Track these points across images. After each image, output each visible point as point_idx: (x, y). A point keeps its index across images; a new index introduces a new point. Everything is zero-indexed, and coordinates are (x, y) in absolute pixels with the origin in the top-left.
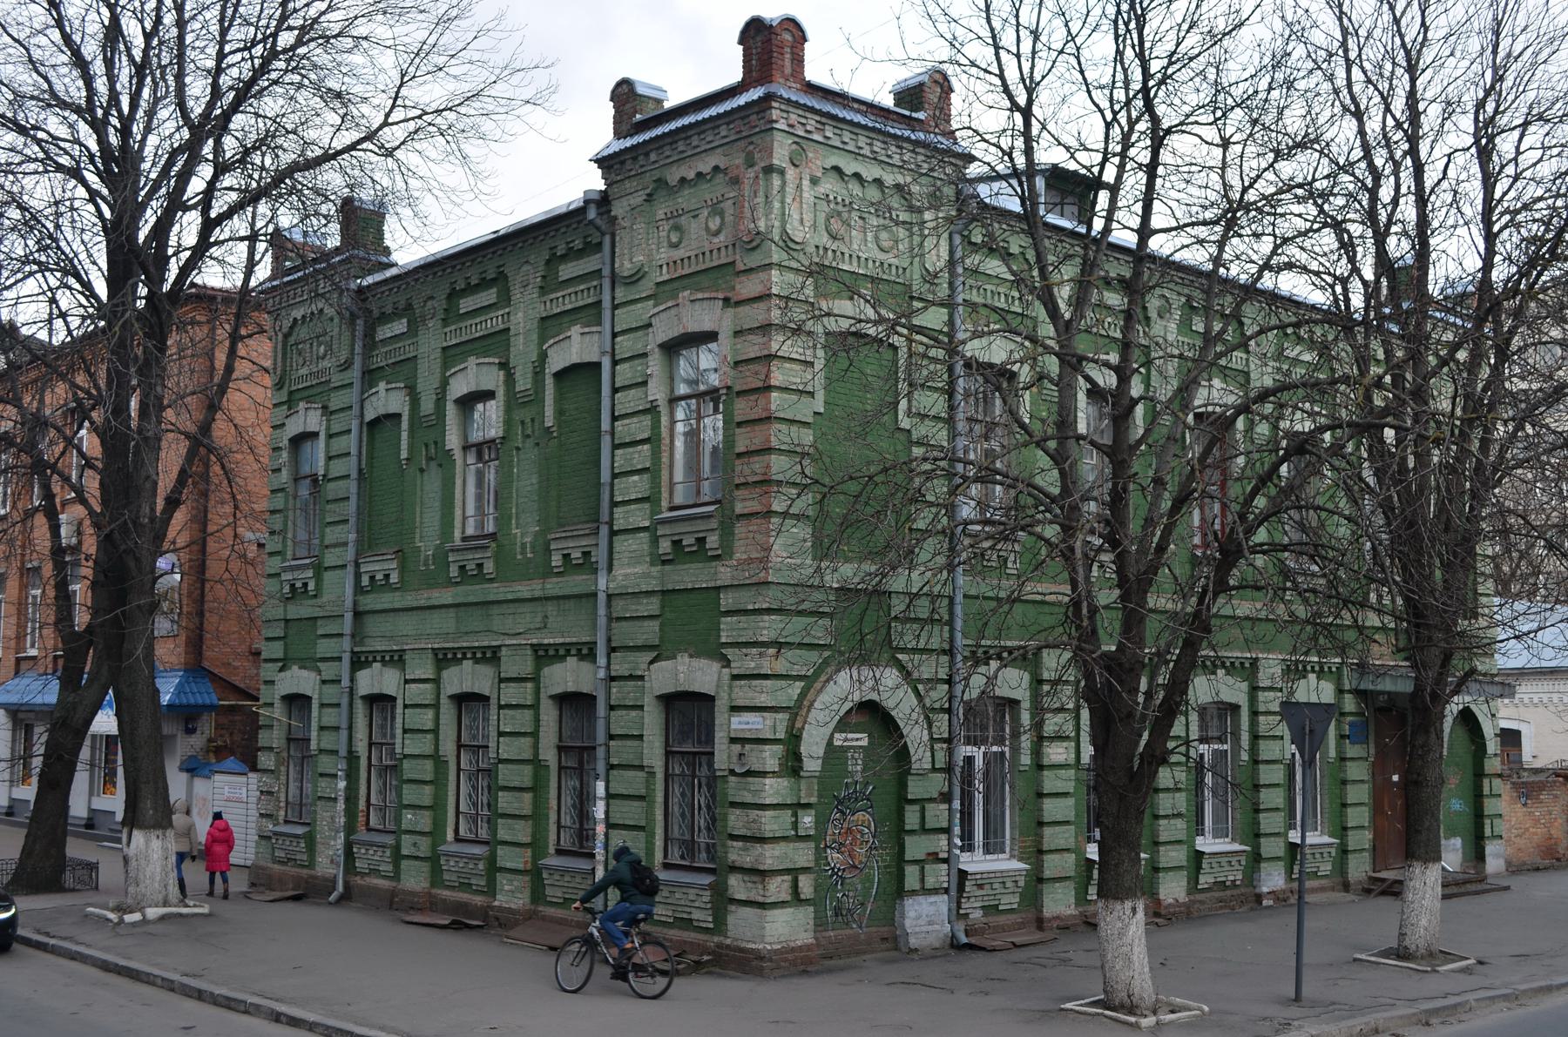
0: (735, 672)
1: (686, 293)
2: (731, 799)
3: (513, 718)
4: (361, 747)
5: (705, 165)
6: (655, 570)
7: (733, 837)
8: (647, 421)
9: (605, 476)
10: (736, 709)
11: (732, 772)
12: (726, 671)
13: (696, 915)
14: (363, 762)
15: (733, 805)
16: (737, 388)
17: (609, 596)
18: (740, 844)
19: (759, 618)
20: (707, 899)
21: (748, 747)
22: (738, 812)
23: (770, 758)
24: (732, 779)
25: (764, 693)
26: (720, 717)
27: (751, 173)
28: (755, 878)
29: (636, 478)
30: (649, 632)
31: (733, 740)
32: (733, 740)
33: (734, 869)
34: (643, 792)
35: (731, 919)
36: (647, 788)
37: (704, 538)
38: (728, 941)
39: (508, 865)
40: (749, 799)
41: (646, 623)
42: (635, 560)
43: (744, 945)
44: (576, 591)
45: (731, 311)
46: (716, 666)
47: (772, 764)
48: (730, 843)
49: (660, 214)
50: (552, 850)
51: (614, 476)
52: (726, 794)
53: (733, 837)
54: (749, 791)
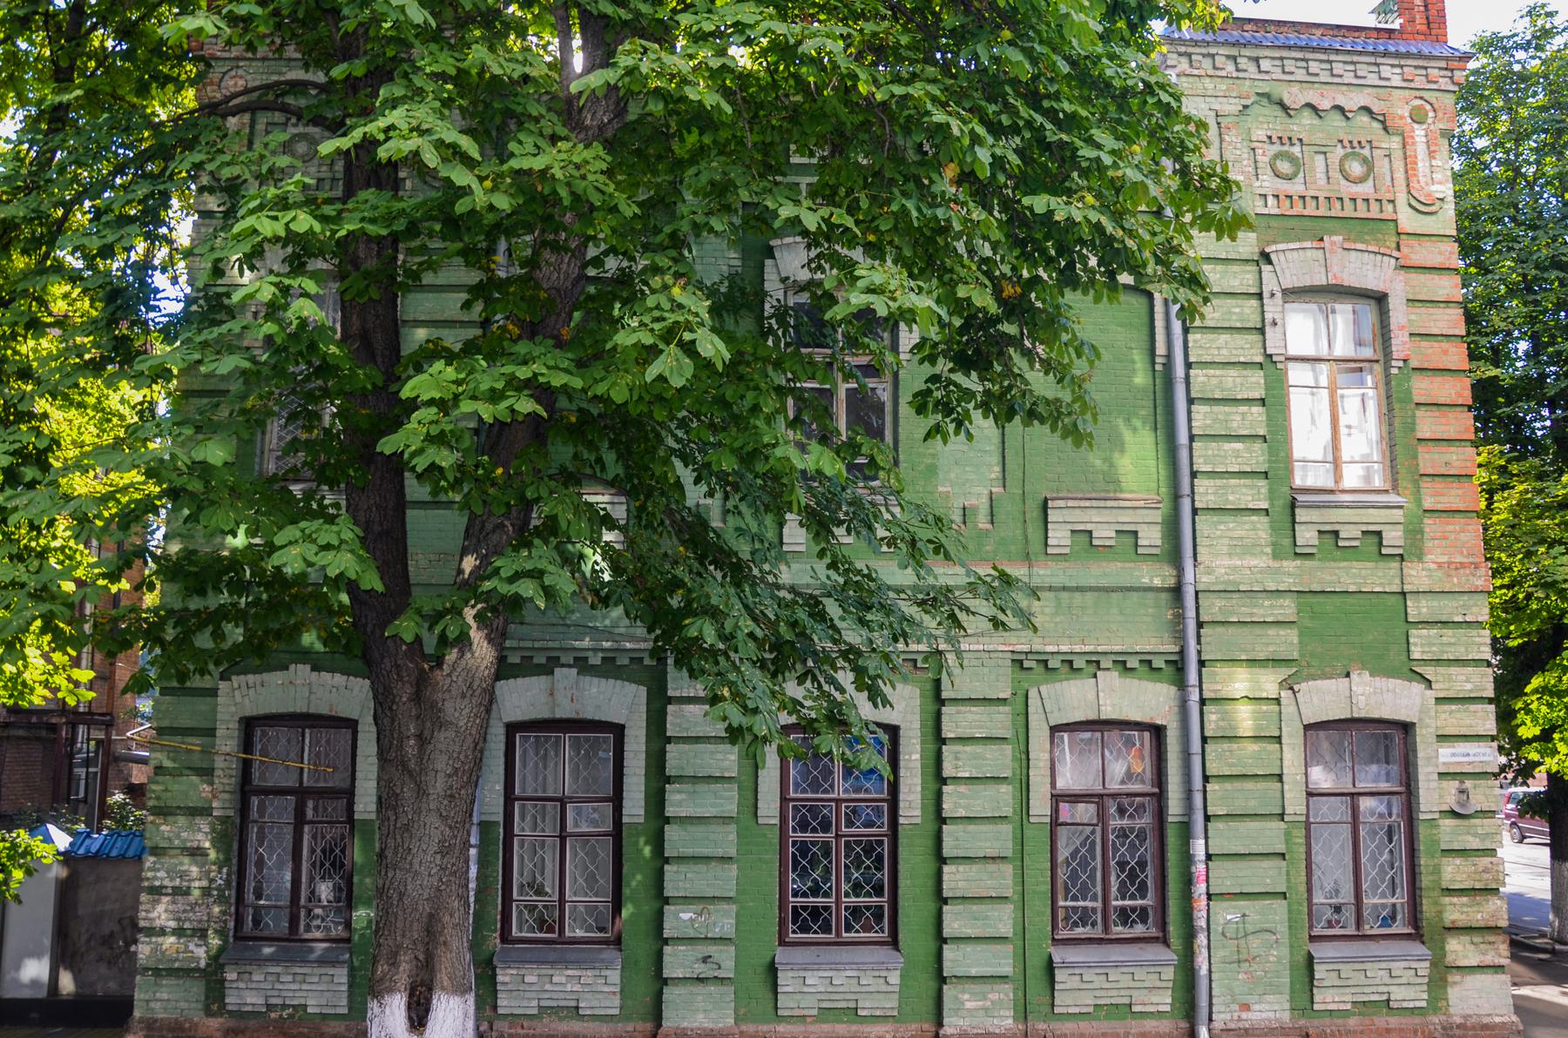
1: (1335, 238)
3: (975, 757)
5: (1352, 100)
6: (1290, 565)
7: (1450, 892)
8: (1257, 377)
9: (1183, 438)
11: (1454, 814)
12: (1429, 692)
13: (1398, 994)
16: (1414, 363)
18: (1465, 899)
19: (1474, 632)
20: (1426, 972)
21: (1468, 784)
22: (1458, 861)
27: (1419, 132)
28: (1492, 938)
29: (1238, 446)
30: (1286, 642)
33: (1454, 929)
34: (1281, 848)
35: (1453, 993)
36: (1287, 842)
38: (1458, 1020)
39: (974, 972)
40: (1474, 843)
41: (1272, 631)
42: (1243, 548)
43: (1486, 1020)
44: (1104, 582)
45: (1402, 275)
46: (1417, 688)
48: (1447, 900)
49: (1260, 134)
51: (1192, 438)
52: (1438, 842)
53: (1450, 892)
54: (1475, 835)
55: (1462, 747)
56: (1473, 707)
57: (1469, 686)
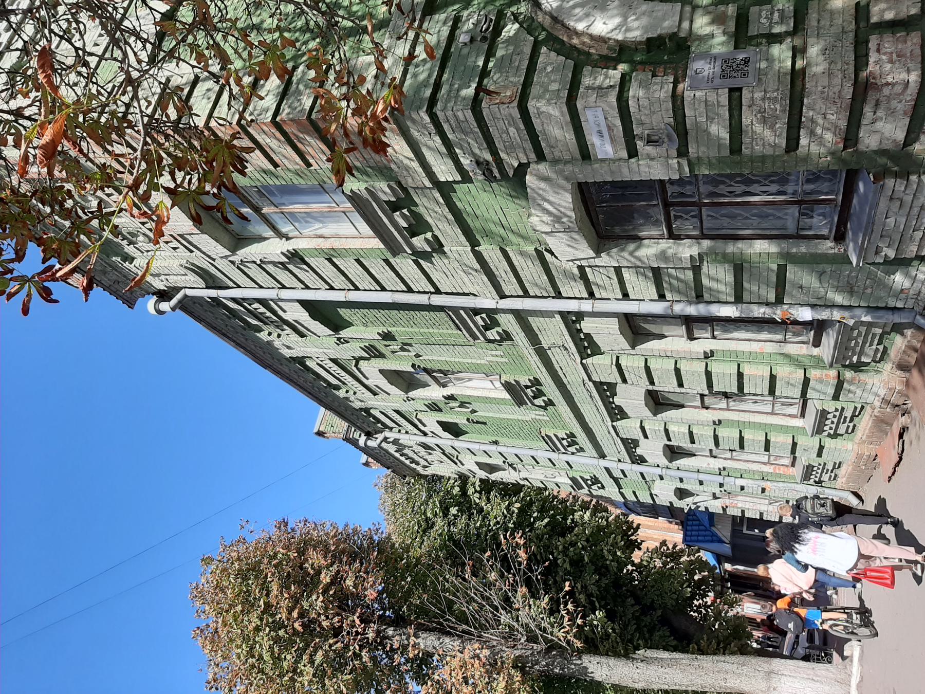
0: (533, 156)
2: (726, 152)
4: (716, 464)
10: (585, 154)
14: (729, 464)
15: (736, 145)
17: (503, 296)
21: (637, 130)
23: (650, 96)
24: (692, 150)
25: (549, 112)
26: (602, 175)
31: (633, 153)
32: (633, 153)
37: (388, 203)
47: (662, 89)
50: (816, 351)
55: (593, 139)
56: (538, 128)
57: (512, 130)
